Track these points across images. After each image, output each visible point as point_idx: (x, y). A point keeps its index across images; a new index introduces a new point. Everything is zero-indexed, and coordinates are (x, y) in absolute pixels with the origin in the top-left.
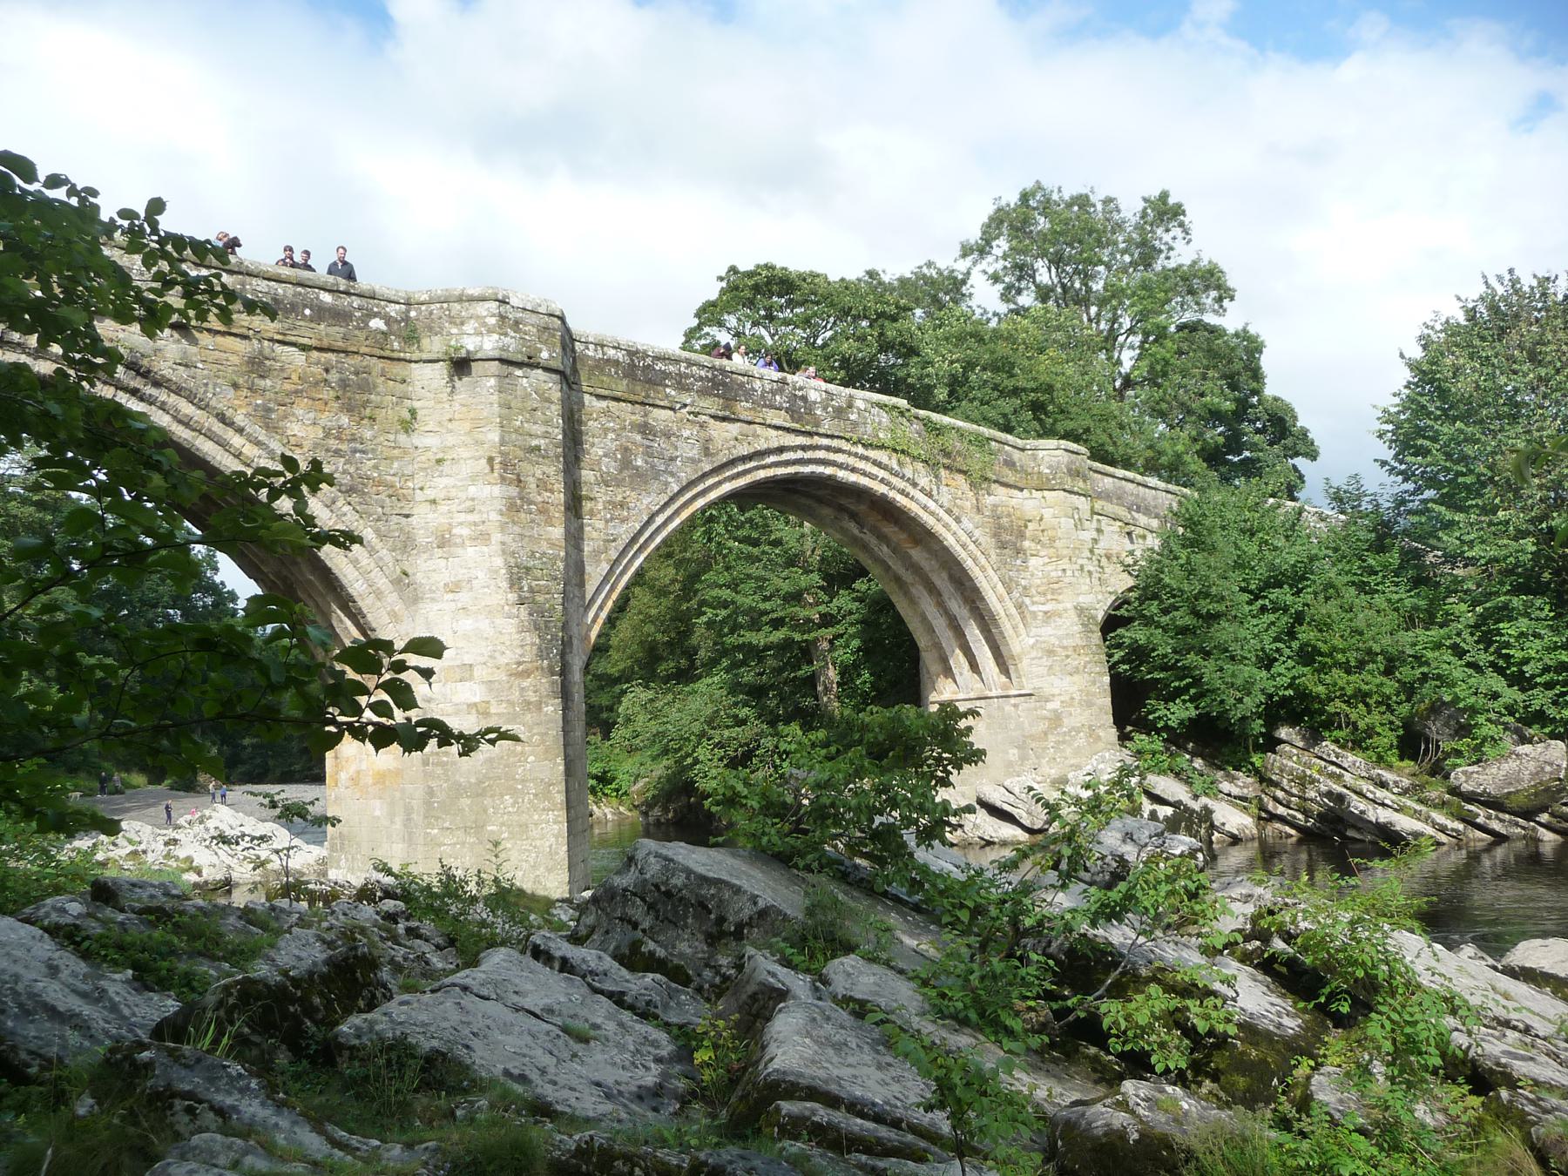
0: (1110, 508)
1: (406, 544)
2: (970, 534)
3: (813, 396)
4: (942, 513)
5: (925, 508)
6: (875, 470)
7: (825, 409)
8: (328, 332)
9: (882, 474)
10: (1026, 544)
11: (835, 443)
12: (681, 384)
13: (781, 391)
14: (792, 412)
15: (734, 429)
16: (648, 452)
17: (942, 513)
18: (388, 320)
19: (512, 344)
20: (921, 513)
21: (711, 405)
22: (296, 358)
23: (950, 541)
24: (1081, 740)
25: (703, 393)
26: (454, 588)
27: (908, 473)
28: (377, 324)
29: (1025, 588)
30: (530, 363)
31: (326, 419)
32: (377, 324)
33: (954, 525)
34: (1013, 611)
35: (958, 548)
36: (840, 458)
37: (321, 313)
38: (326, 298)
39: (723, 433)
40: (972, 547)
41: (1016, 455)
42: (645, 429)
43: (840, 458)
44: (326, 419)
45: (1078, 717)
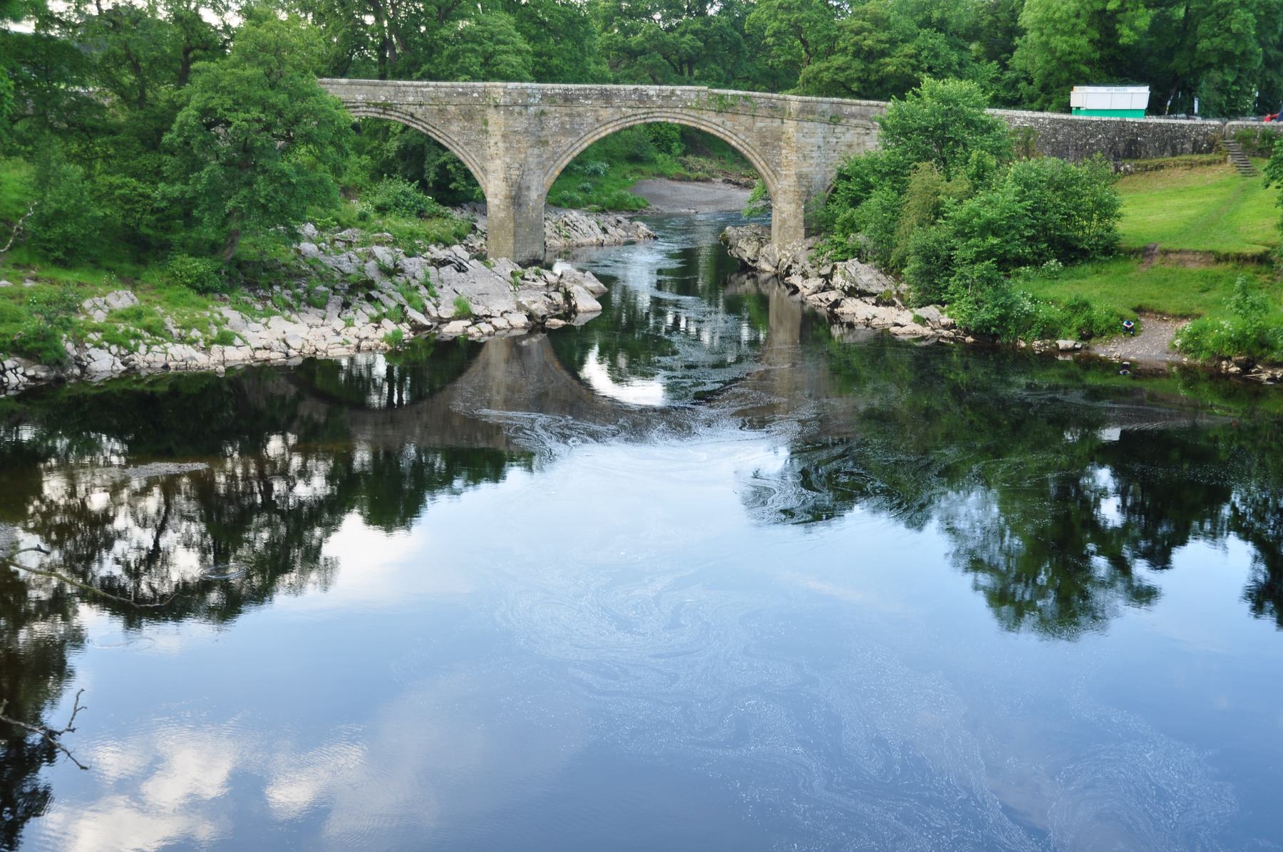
0: (854, 121)
1: (484, 158)
2: (744, 141)
3: (651, 93)
4: (727, 133)
5: (717, 131)
6: (687, 118)
7: (658, 96)
8: (462, 100)
9: (692, 119)
10: (782, 144)
11: (664, 109)
12: (586, 97)
13: (635, 93)
14: (640, 101)
15: (610, 110)
16: (571, 123)
17: (727, 133)
18: (478, 93)
19: (508, 99)
20: (715, 133)
21: (600, 103)
22: (453, 108)
23: (733, 143)
24: (792, 232)
25: (596, 99)
26: (494, 172)
27: (705, 117)
28: (475, 95)
29: (777, 163)
30: (516, 104)
31: (461, 124)
32: (475, 95)
33: (734, 137)
34: (770, 173)
35: (739, 147)
36: (668, 115)
37: (459, 94)
38: (460, 90)
39: (606, 113)
40: (746, 146)
41: (779, 103)
42: (570, 115)
43: (668, 115)
44: (461, 124)
45: (792, 222)
